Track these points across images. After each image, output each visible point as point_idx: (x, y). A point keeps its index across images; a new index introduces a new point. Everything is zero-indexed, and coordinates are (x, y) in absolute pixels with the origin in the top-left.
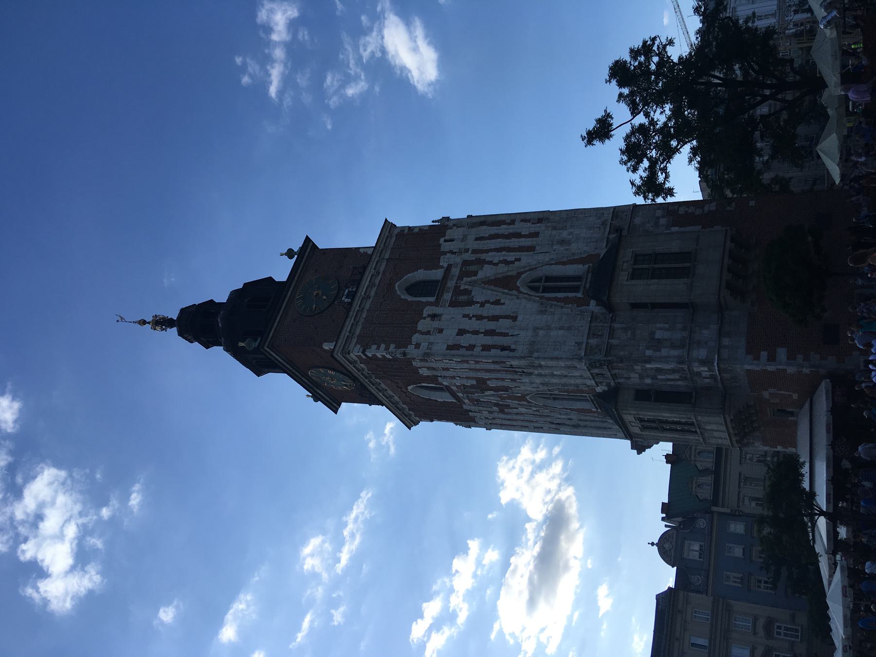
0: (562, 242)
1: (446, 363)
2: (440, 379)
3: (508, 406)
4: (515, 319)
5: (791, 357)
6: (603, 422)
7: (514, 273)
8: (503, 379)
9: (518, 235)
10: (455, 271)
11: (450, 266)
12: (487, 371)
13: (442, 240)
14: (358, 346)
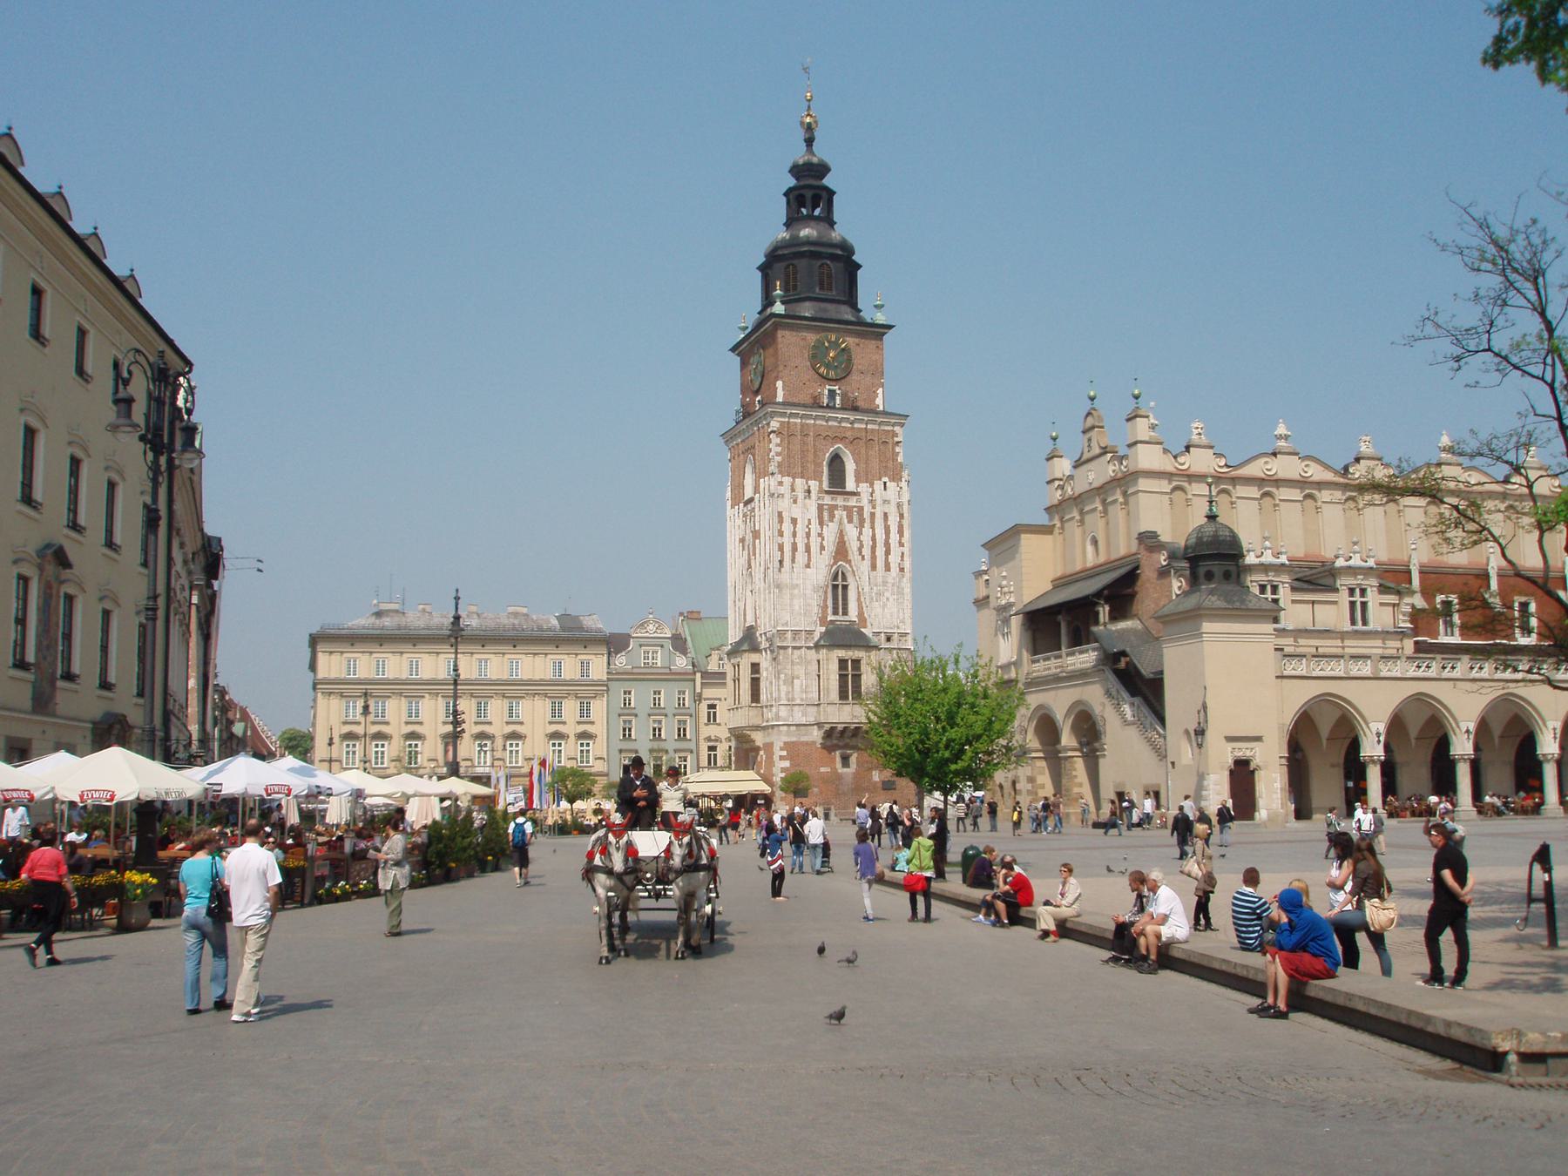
0: (879, 594)
1: (769, 509)
4: (808, 566)
5: (783, 770)
7: (850, 557)
9: (888, 552)
10: (852, 502)
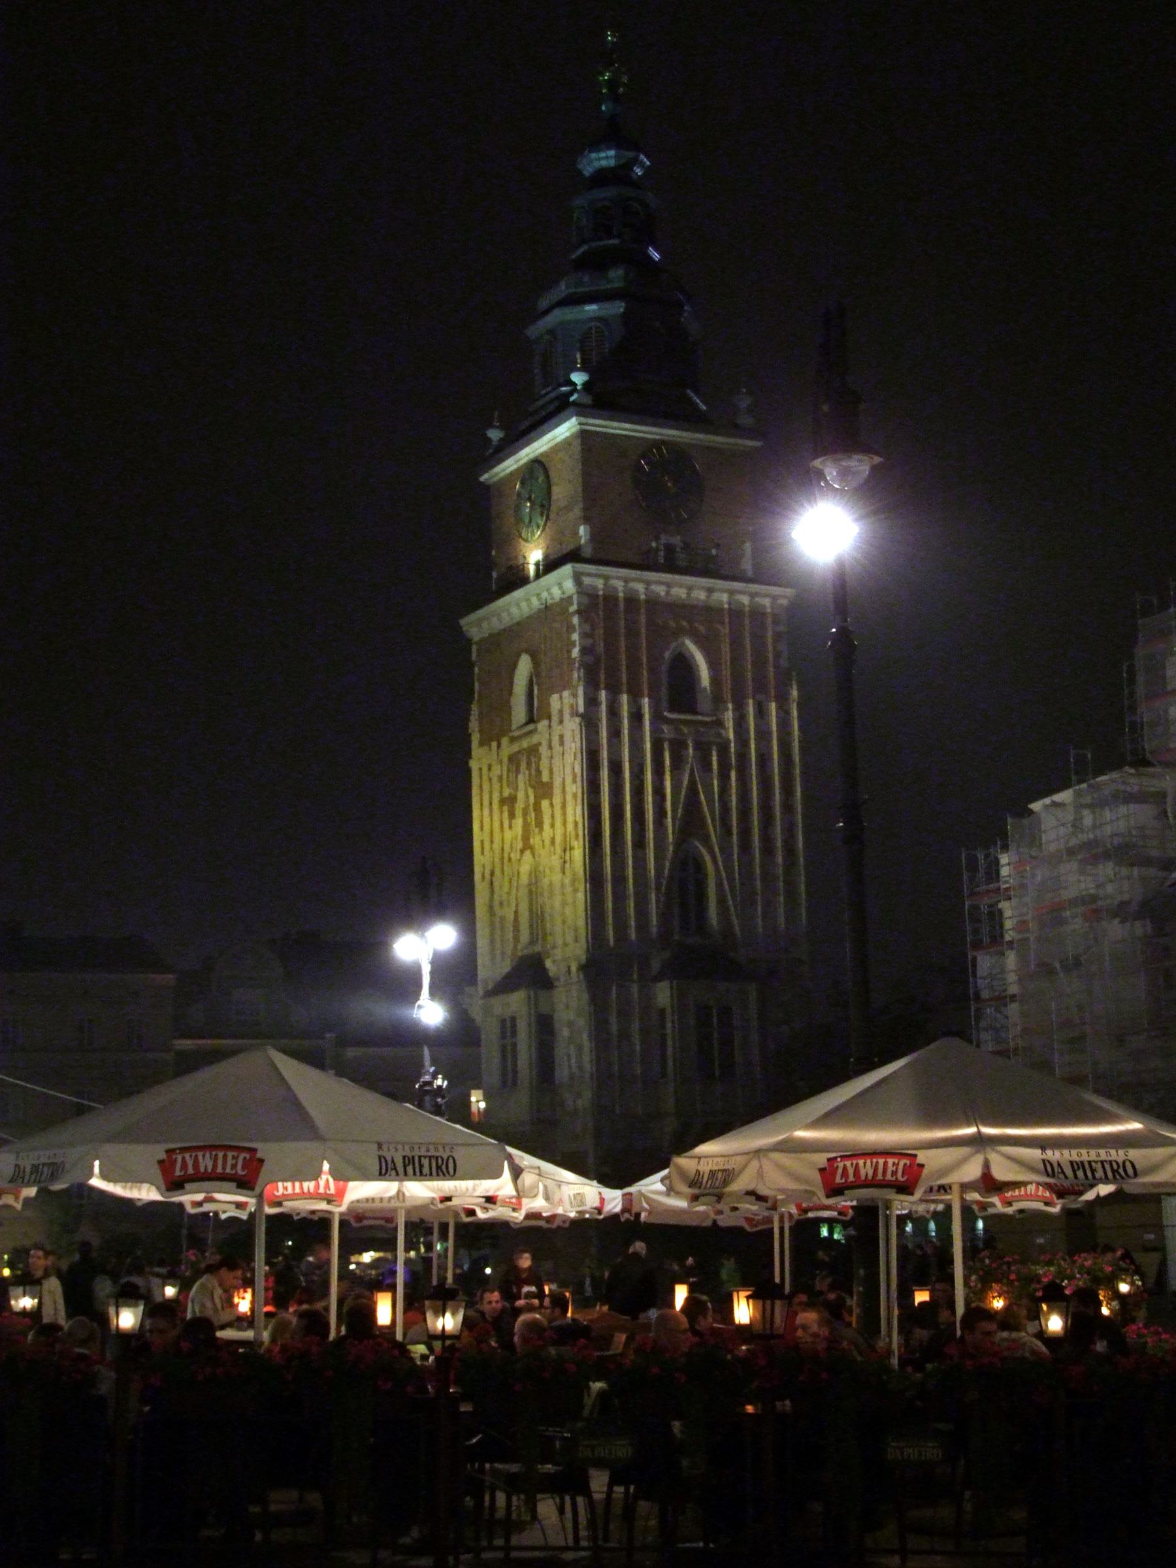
2: (545, 722)
3: (512, 815)
6: (503, 953)
8: (553, 826)
11: (720, 723)
12: (564, 807)
13: (761, 697)
14: (586, 600)
